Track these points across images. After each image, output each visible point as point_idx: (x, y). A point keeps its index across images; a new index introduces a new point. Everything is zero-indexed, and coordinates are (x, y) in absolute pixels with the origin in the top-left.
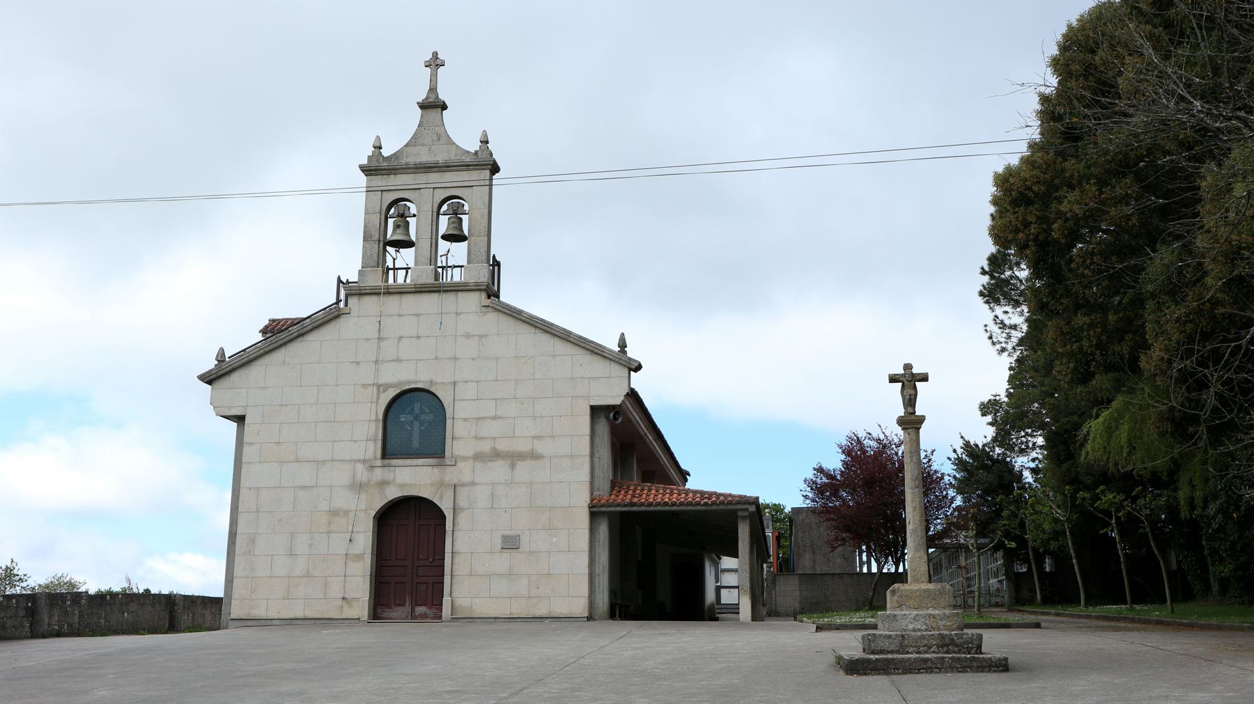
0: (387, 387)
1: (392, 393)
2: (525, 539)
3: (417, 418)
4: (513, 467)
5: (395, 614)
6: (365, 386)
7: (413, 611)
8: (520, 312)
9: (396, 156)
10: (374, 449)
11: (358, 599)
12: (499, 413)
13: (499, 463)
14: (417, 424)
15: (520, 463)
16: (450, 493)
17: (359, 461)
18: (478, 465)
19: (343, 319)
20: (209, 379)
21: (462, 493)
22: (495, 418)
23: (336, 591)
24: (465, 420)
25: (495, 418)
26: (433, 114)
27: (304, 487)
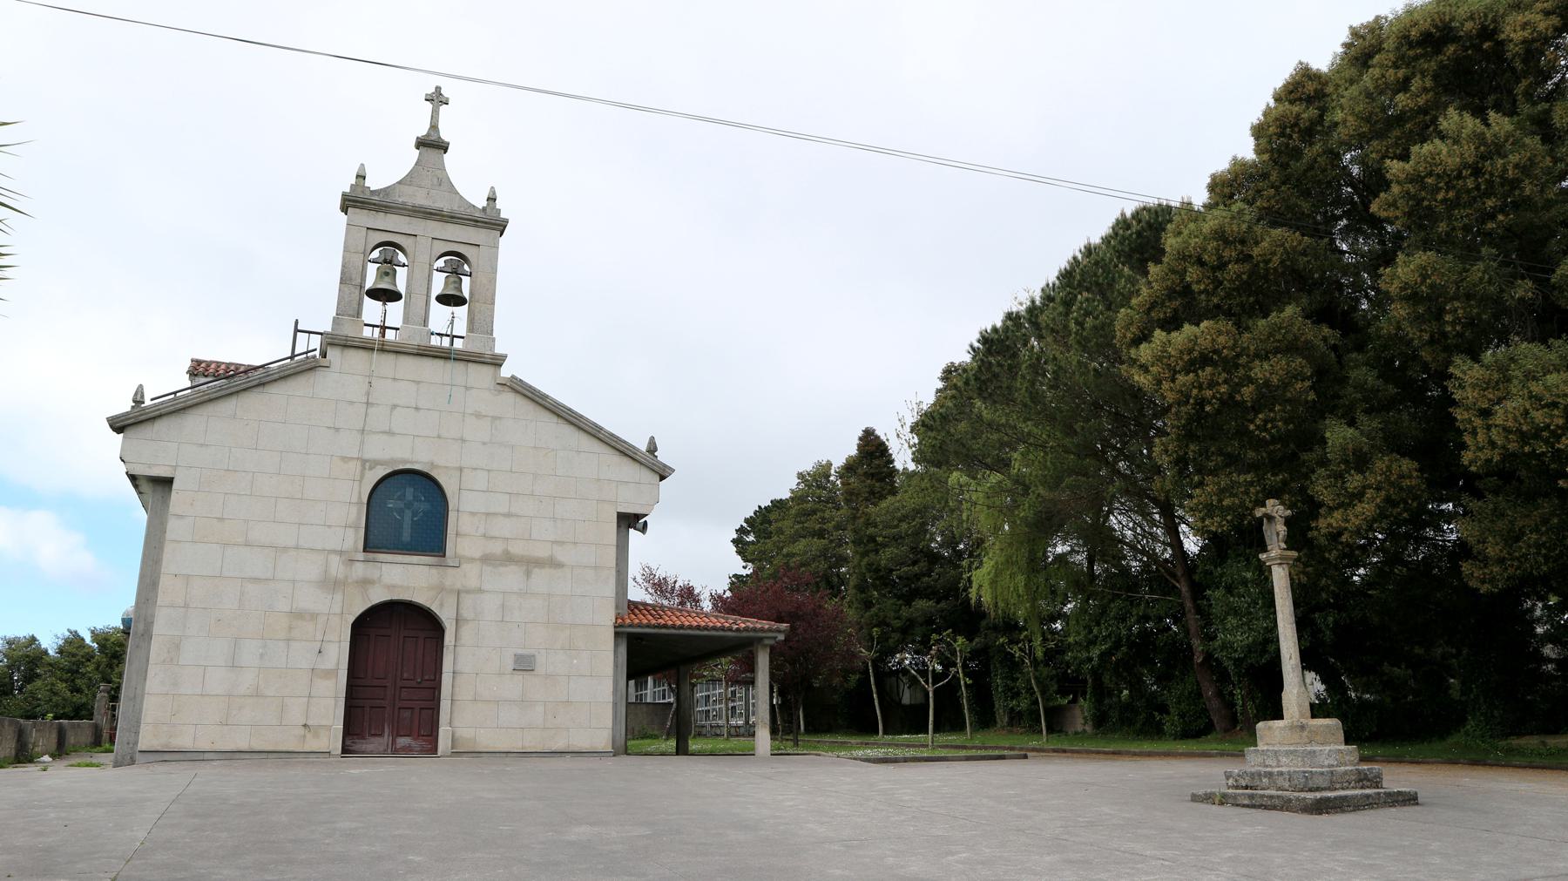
0: (375, 463)
1: (382, 472)
2: (541, 660)
3: (409, 505)
4: (528, 574)
5: (370, 747)
6: (345, 459)
7: (394, 742)
8: (545, 397)
9: (386, 191)
10: (355, 538)
11: (329, 728)
12: (513, 510)
13: (513, 568)
14: (408, 513)
15: (536, 571)
16: (452, 600)
17: (334, 552)
18: (487, 569)
19: (320, 373)
20: (119, 425)
21: (467, 601)
22: (508, 515)
23: (296, 716)
24: (473, 514)
25: (508, 515)
26: (432, 154)
27: (256, 580)
